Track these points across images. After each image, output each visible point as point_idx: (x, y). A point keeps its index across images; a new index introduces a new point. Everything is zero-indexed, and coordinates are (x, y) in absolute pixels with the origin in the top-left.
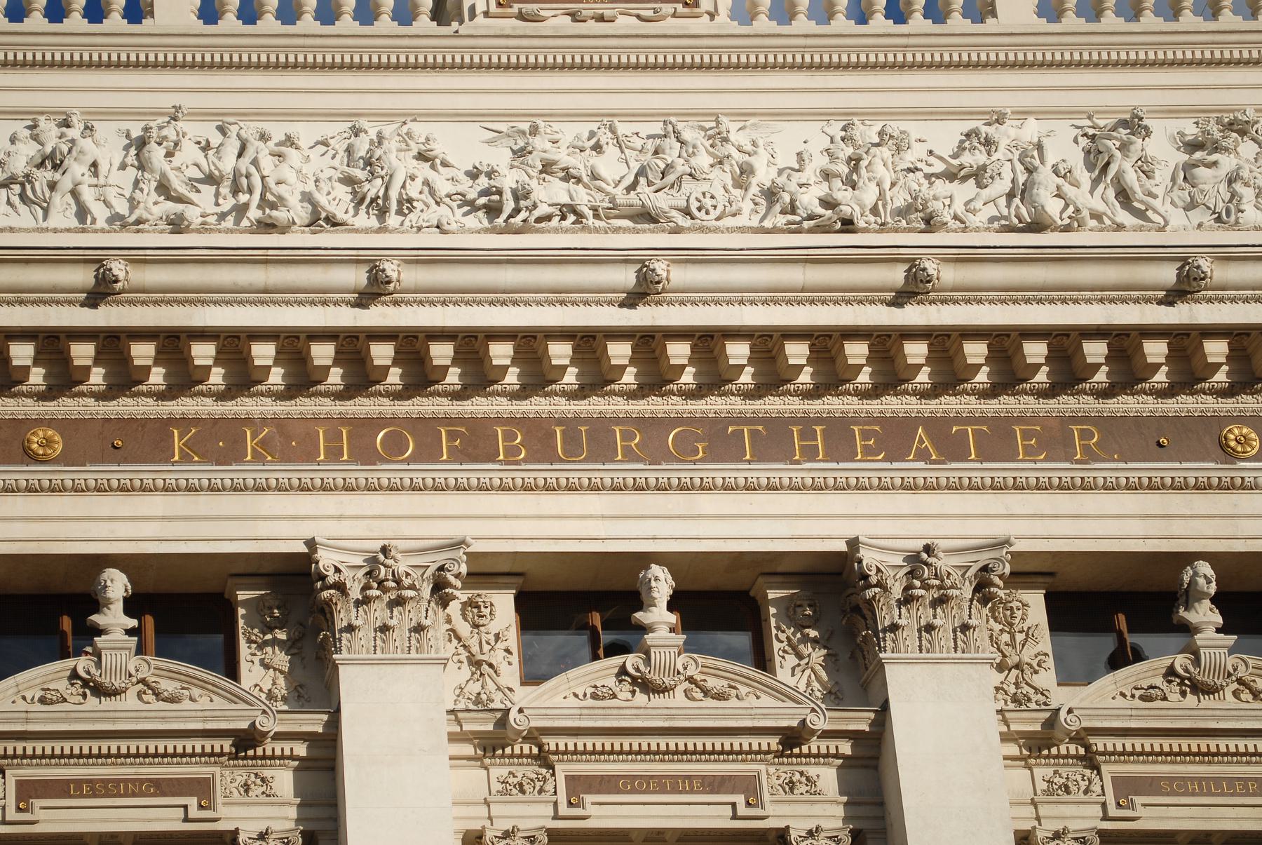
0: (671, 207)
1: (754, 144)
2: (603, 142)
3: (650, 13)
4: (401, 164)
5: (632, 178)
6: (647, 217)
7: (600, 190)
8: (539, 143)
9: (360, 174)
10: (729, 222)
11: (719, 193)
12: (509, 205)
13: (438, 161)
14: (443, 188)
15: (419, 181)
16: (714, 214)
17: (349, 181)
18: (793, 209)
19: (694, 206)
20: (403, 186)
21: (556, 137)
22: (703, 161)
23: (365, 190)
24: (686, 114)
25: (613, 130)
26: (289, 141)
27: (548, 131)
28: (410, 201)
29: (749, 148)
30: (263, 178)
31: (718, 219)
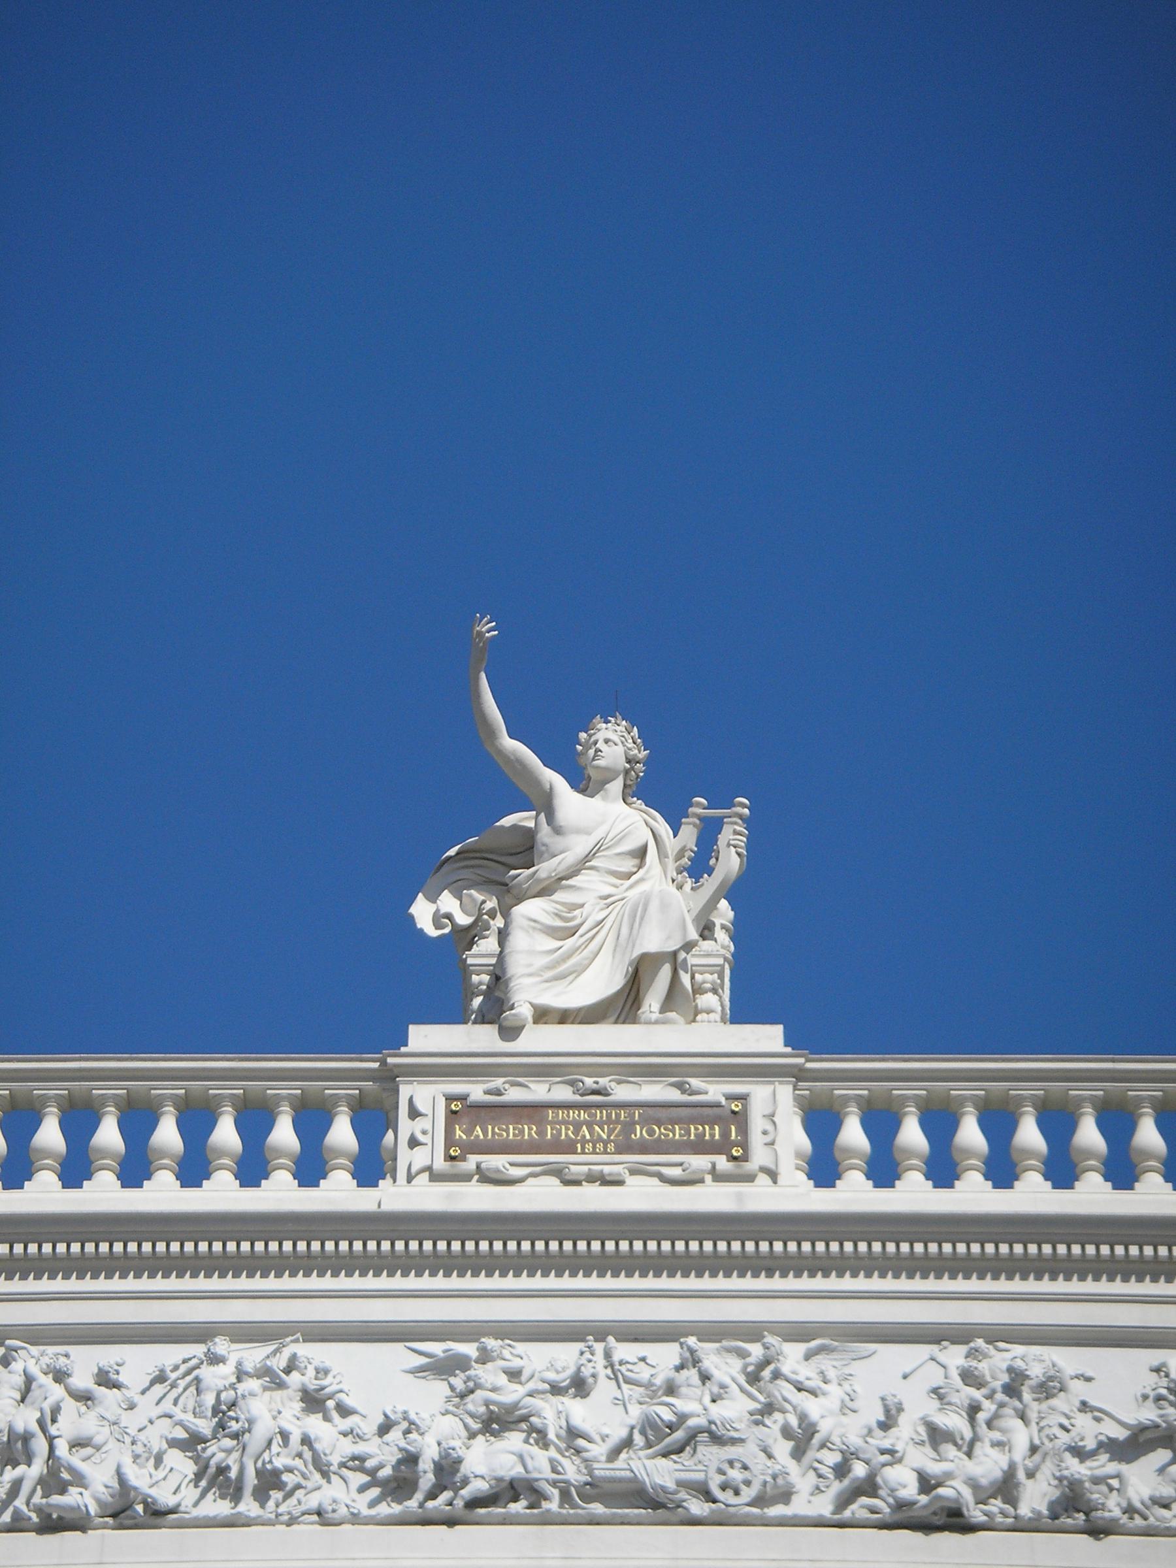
0: (680, 1484)
2: (586, 1372)
3: (675, 1172)
4: (270, 1412)
5: (623, 1433)
7: (578, 1452)
8: (489, 1374)
9: (205, 1426)
11: (758, 1462)
13: (330, 1404)
15: (295, 1439)
16: (748, 1494)
17: (192, 1443)
18: (869, 1487)
21: (516, 1363)
23: (209, 1452)
24: (713, 1332)
25: (608, 1355)
26: (105, 1379)
27: (506, 1353)
28: (276, 1473)
29: (815, 1383)
30: (51, 1440)
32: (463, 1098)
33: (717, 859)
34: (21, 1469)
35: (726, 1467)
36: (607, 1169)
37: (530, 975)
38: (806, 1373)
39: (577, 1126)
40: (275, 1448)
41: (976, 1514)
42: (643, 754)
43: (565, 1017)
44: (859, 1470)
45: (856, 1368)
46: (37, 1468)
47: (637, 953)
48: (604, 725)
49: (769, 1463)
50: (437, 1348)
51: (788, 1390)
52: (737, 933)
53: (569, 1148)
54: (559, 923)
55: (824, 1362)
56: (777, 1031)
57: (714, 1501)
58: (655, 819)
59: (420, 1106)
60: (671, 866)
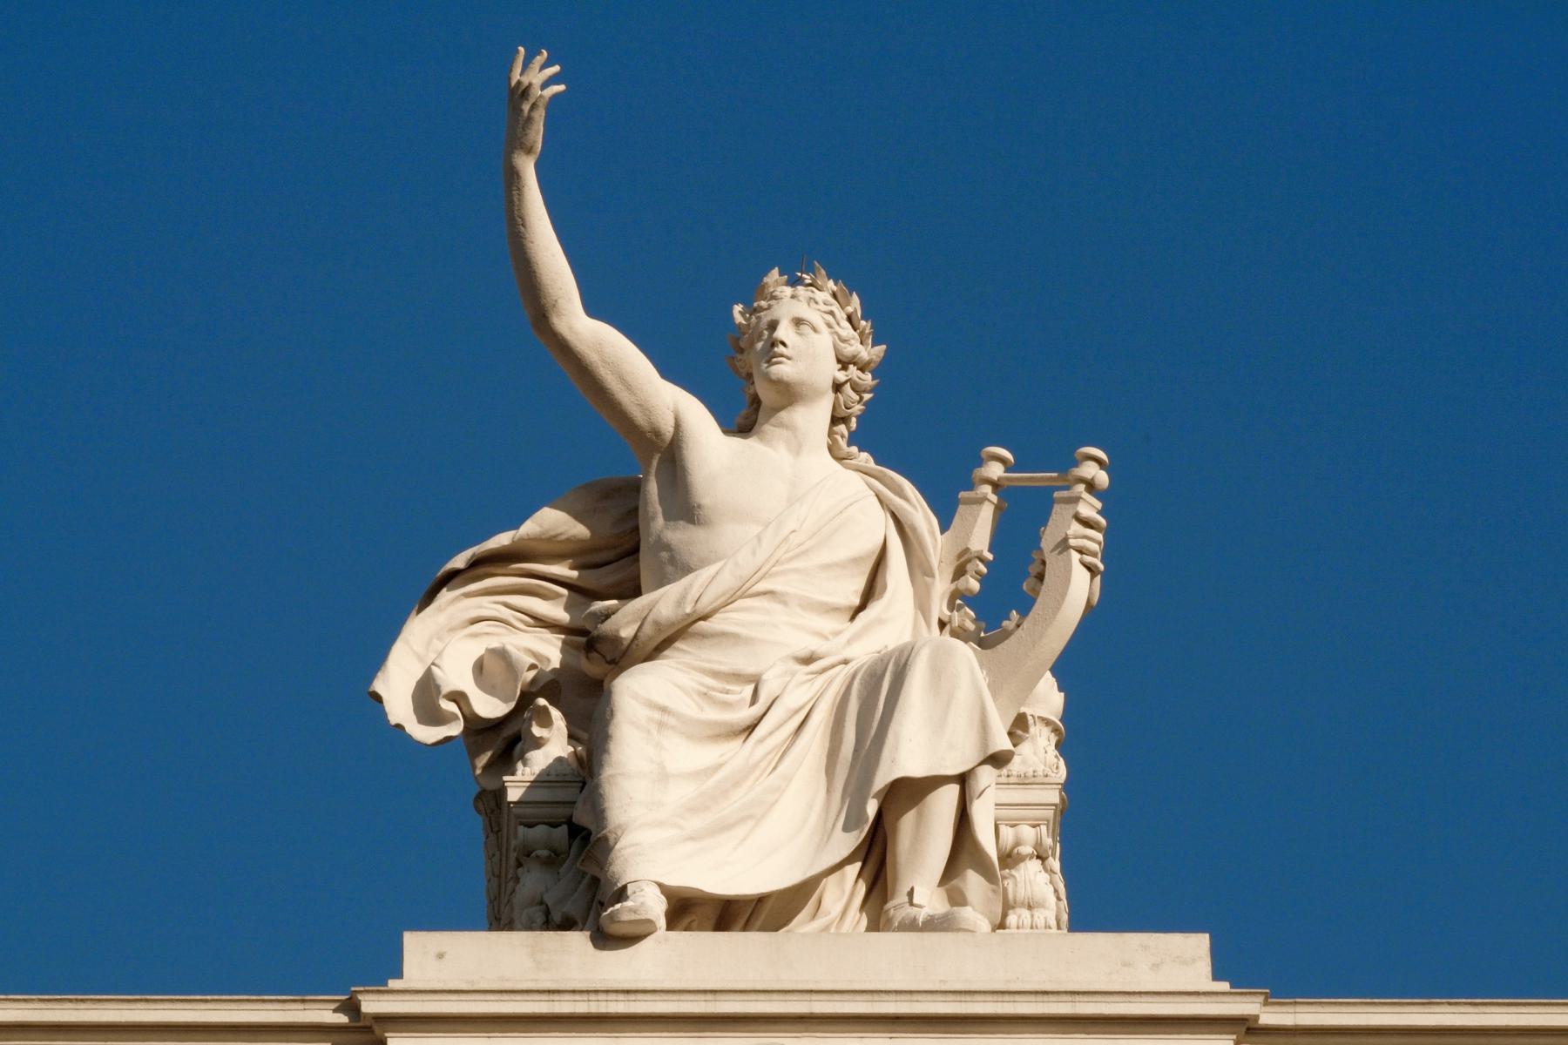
33: (1041, 577)
37: (660, 824)
42: (871, 353)
43: (727, 914)
47: (882, 780)
48: (788, 291)
52: (1073, 739)
54: (713, 714)
56: (1198, 945)
58: (900, 493)
60: (941, 586)
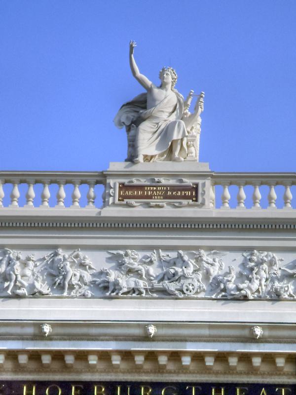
0: (177, 290)
1: (214, 260)
6: (165, 293)
10: (199, 296)
11: (196, 284)
12: (111, 288)
13: (87, 267)
14: (88, 277)
18: (224, 290)
19: (185, 289)
20: (71, 279)
22: (190, 270)
24: (186, 248)
25: (158, 254)
27: (133, 254)
30: (16, 275)
31: (197, 293)
32: (123, 184)
34: (9, 283)
35: (188, 285)
36: (160, 204)
38: (210, 260)
39: (153, 191)
40: (73, 279)
41: (251, 297)
44: (222, 286)
45: (223, 258)
46: (12, 284)
49: (199, 284)
50: (115, 252)
51: (206, 265)
53: (150, 197)
55: (215, 256)
56: (208, 163)
57: (185, 294)
59: (112, 185)
